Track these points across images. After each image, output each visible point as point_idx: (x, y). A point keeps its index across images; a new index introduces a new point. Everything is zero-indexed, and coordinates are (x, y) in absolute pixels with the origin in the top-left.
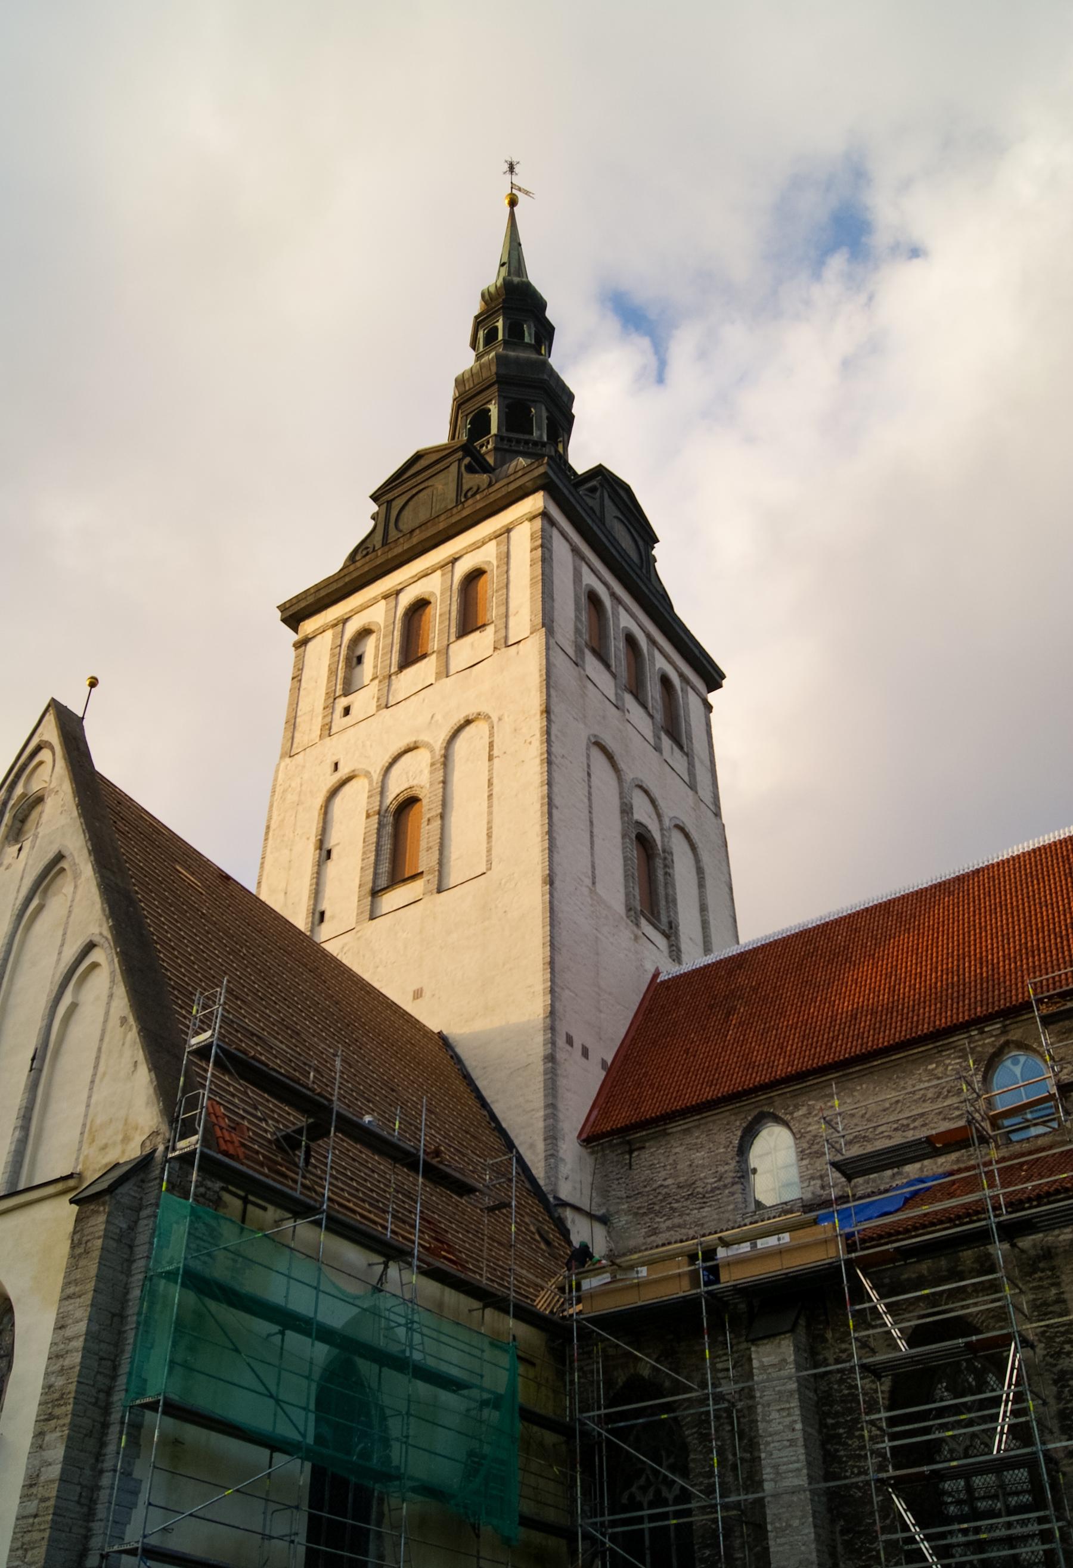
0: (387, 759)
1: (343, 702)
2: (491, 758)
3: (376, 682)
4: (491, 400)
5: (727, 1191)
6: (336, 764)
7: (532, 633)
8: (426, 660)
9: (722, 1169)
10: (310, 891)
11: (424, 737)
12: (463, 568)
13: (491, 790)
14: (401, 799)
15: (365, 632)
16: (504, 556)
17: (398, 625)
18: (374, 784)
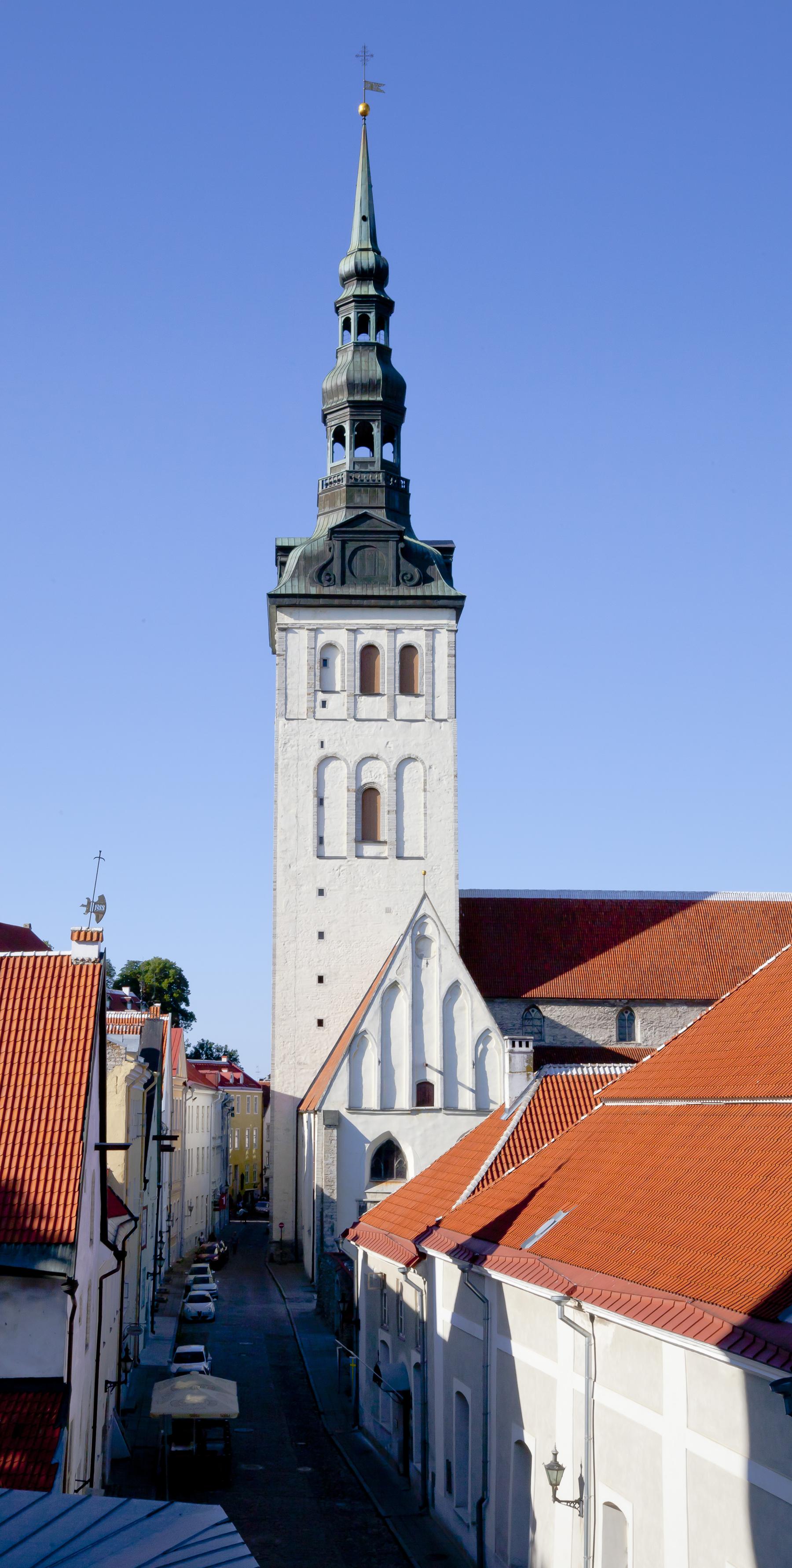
0: (357, 758)
1: (321, 696)
2: (425, 790)
3: (345, 694)
4: (374, 421)
5: (516, 1031)
6: (322, 743)
7: (449, 718)
8: (378, 698)
9: (515, 1022)
10: (314, 822)
11: (382, 755)
12: (403, 639)
13: (426, 811)
14: (367, 786)
15: (330, 646)
16: (431, 648)
17: (358, 658)
18: (351, 770)
